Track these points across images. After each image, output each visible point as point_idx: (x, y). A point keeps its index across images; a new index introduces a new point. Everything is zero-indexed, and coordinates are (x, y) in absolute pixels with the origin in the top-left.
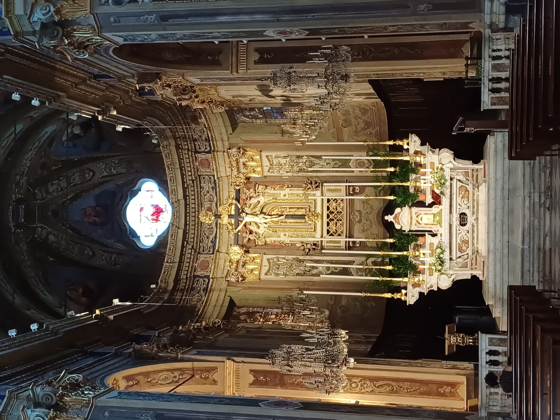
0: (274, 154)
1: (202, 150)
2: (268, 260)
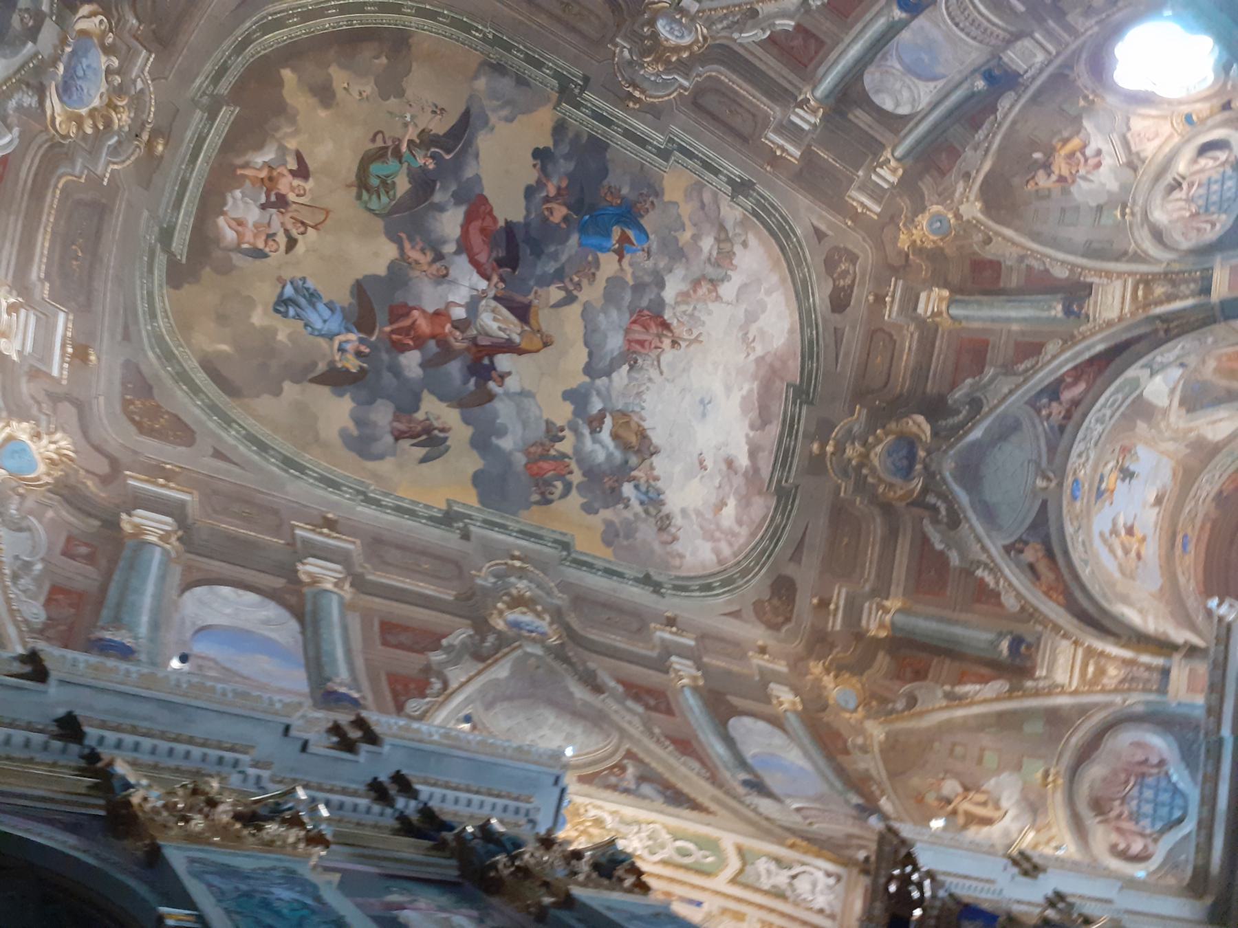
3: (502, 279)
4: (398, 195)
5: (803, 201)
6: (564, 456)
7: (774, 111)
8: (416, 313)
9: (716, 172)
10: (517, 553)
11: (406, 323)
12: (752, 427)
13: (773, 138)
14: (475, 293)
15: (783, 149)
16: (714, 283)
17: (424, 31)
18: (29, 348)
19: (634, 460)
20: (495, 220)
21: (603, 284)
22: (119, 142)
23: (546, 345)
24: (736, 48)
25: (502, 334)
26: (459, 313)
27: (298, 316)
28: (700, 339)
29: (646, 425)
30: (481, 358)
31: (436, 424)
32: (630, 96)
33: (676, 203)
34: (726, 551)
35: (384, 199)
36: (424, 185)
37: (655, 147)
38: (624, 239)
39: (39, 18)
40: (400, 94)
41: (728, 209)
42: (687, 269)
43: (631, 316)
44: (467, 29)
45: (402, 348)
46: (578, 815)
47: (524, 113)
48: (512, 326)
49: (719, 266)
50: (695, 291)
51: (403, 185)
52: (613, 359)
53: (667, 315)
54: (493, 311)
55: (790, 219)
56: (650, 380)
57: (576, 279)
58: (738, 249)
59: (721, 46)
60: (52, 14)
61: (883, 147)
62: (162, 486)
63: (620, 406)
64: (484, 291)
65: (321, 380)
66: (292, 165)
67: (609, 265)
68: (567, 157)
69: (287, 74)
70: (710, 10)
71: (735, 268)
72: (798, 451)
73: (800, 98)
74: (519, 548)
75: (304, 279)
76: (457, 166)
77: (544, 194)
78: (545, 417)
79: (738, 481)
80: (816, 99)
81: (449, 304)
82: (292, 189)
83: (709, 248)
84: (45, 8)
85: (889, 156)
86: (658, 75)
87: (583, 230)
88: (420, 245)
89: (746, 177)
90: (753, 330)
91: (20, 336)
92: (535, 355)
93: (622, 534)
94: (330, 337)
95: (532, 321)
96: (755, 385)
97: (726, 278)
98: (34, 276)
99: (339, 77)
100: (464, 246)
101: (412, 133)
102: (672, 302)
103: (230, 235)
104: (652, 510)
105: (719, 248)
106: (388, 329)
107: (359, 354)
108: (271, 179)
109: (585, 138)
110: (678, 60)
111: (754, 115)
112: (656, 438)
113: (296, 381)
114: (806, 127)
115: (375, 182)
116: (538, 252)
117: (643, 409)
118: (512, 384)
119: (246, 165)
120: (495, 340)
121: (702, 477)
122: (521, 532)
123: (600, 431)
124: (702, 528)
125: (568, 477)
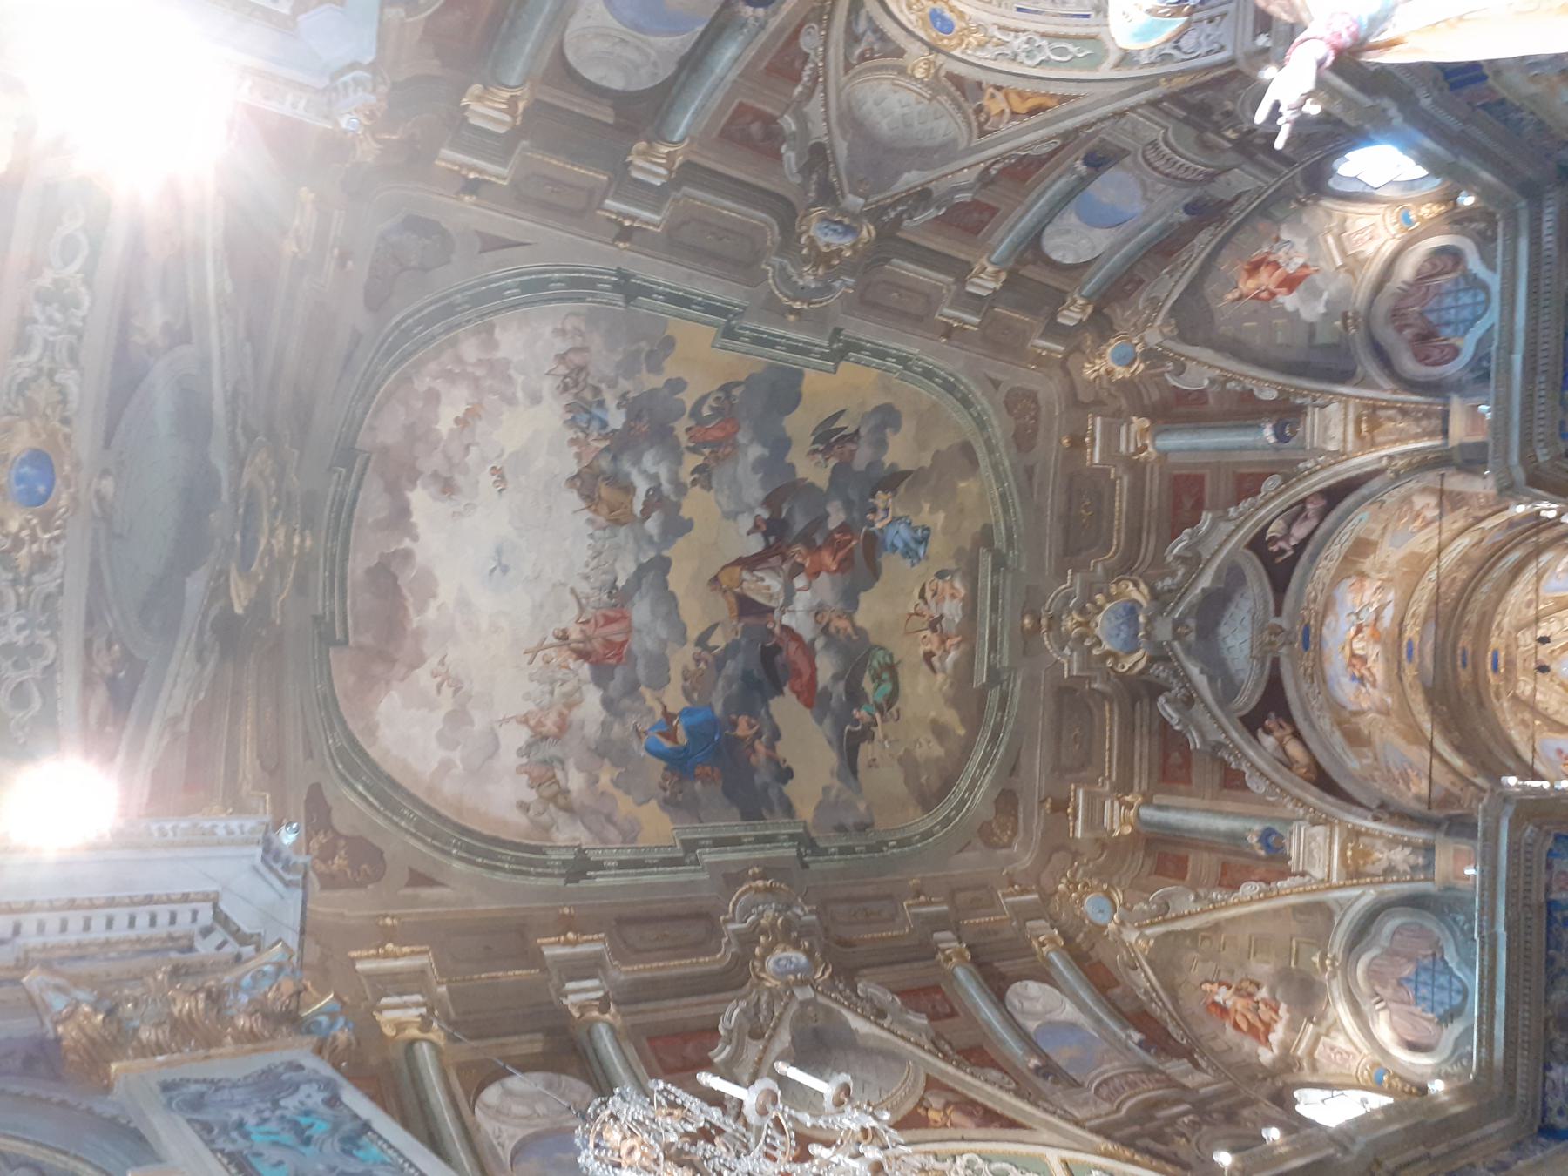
3: (771, 632)
4: (867, 673)
5: (487, 905)
6: (694, 450)
7: (623, 973)
8: (834, 568)
9: (623, 865)
10: (792, 318)
11: (840, 555)
12: (407, 555)
13: (592, 946)
14: (790, 608)
15: (568, 943)
16: (540, 738)
17: (920, 822)
18: (1123, 430)
19: (605, 463)
20: (794, 691)
21: (672, 674)
22: (1067, 604)
23: (715, 579)
24: (729, 995)
25: (760, 574)
26: (800, 582)
27: (915, 530)
28: (529, 656)
29: (588, 514)
30: (777, 540)
31: (819, 457)
32: (764, 877)
33: (640, 804)
34: (470, 350)
35: (875, 663)
36: (855, 696)
37: (704, 847)
38: (670, 735)
39: (1177, 636)
40: (900, 760)
41: (577, 834)
42: (583, 738)
43: (629, 651)
44: (901, 843)
45: (844, 528)
47: (821, 802)
48: (752, 586)
49: (545, 762)
50: (561, 715)
51: (867, 684)
52: (639, 587)
53: (585, 669)
54: (771, 597)
55: (486, 874)
56: (587, 578)
57: (702, 665)
58: (531, 796)
59: (743, 984)
60: (1169, 644)
61: (451, 1038)
62: (1044, 349)
63: (623, 531)
64: (783, 613)
65: (906, 474)
66: (935, 660)
67: (675, 699)
68: (765, 787)
69: (962, 732)
70: (787, 1004)
71: (520, 770)
72: (323, 534)
73: (613, 1008)
74: (786, 326)
75: (913, 565)
76: (839, 725)
77: (764, 738)
78: (712, 492)
79: (431, 463)
80: (596, 1020)
81: (808, 587)
82: (930, 641)
83: (570, 777)
84: (1176, 644)
85: (431, 1036)
86: (760, 915)
87: (714, 722)
88: (841, 636)
89: (583, 883)
90: (447, 702)
91: (1132, 435)
92: (726, 562)
93: (643, 356)
94: (895, 520)
95: (733, 600)
96: (415, 621)
97: (526, 751)
98: (1126, 480)
99: (938, 751)
100: (809, 651)
101: (879, 732)
102: (584, 688)
103: (958, 584)
104: (588, 395)
105: (557, 782)
106: (854, 543)
107: (874, 510)
108: (943, 642)
109: (765, 812)
110: (757, 942)
111: (638, 951)
112: (573, 499)
113: (921, 468)
114: (570, 986)
115: (885, 676)
116: (746, 676)
117: (591, 536)
118: (746, 522)
119: (959, 643)
120: (765, 565)
121: (499, 456)
122: (773, 345)
123: (648, 491)
124: (509, 380)
125: (692, 423)
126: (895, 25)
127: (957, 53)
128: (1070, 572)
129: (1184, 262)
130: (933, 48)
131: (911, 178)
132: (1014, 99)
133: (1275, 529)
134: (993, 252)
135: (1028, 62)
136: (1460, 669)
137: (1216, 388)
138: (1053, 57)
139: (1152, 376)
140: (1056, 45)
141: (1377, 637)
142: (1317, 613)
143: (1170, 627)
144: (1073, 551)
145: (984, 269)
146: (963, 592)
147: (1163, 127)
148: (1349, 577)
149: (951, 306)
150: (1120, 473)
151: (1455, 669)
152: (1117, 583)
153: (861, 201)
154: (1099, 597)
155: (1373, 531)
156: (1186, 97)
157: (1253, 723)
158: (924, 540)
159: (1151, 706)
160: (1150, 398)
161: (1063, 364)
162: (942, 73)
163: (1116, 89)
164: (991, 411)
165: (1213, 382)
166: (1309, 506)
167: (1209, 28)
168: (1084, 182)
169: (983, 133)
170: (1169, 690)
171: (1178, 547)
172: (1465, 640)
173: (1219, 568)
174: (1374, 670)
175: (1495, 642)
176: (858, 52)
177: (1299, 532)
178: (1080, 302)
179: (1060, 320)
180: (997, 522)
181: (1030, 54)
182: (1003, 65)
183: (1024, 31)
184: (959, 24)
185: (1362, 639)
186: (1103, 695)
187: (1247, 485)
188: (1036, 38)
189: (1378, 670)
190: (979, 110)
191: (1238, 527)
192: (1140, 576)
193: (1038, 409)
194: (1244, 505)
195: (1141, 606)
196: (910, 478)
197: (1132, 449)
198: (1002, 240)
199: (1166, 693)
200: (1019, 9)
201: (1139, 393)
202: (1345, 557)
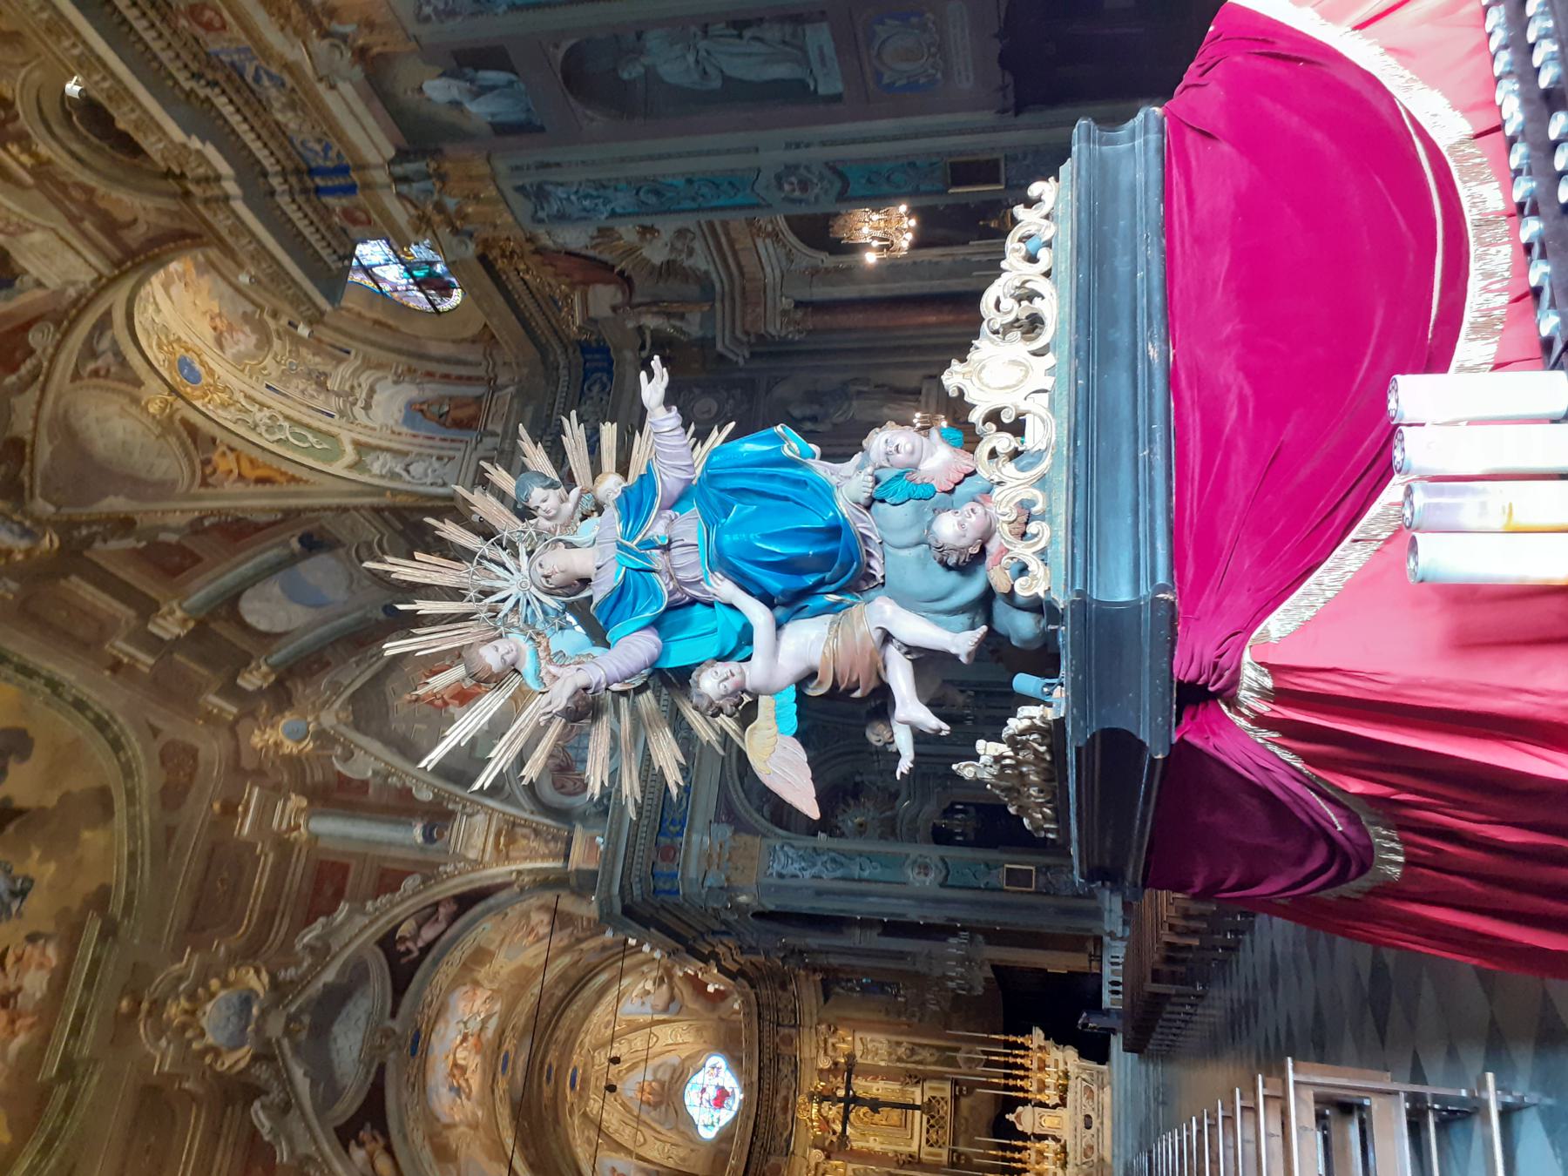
0: (869, 1037)
1: (786, 1022)
2: (854, 1170)
18: (280, 806)
22: (176, 986)
39: (287, 1032)
46: (170, 362)
60: (278, 1041)
62: (215, 706)
65: (20, 812)
91: (287, 812)
113: (42, 810)
126: (139, 357)
127: (198, 404)
128: (188, 950)
129: (372, 657)
130: (173, 390)
131: (116, 503)
132: (245, 465)
133: (406, 930)
134: (187, 598)
135: (267, 436)
136: (544, 1085)
137: (378, 780)
138: (291, 439)
139: (318, 757)
140: (298, 430)
141: (479, 1048)
142: (429, 1018)
143: (283, 1020)
144: (195, 930)
145: (171, 612)
146: (54, 962)
147: (380, 532)
148: (465, 984)
149: (128, 640)
150: (267, 849)
151: (540, 1085)
152: (237, 969)
153: (51, 509)
154: (214, 983)
155: (493, 941)
156: (406, 514)
157: (346, 1135)
158: (22, 894)
159: (243, 1113)
160: (313, 777)
161: (233, 728)
162: (177, 417)
163: (345, 487)
164: (142, 759)
165: (375, 773)
166: (442, 910)
167: (436, 464)
168: (292, 560)
169: (205, 483)
170: (267, 1093)
171: (309, 936)
172: (552, 1058)
173: (345, 964)
174: (471, 1081)
175: (577, 1059)
176: (91, 366)
177: (428, 934)
178: (264, 668)
179: (240, 682)
180: (118, 883)
181: (269, 429)
182: (242, 430)
183: (269, 407)
184: (206, 379)
185: (465, 1049)
186: (193, 1098)
187: (388, 880)
188: (281, 418)
189: (475, 1081)
190: (206, 462)
191: (372, 923)
192: (265, 963)
193: (195, 768)
194: (383, 900)
195: (257, 996)
196: (24, 818)
197: (284, 826)
198: (199, 590)
199: (263, 1098)
200: (268, 387)
201: (304, 770)
202: (464, 964)
